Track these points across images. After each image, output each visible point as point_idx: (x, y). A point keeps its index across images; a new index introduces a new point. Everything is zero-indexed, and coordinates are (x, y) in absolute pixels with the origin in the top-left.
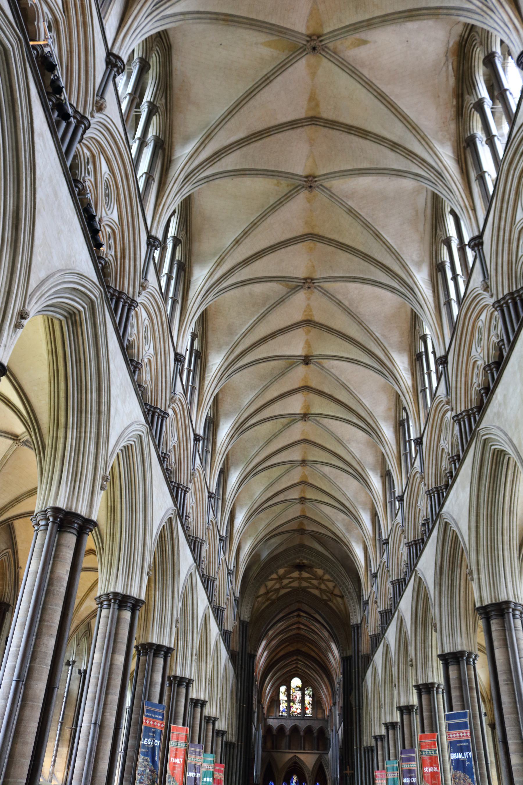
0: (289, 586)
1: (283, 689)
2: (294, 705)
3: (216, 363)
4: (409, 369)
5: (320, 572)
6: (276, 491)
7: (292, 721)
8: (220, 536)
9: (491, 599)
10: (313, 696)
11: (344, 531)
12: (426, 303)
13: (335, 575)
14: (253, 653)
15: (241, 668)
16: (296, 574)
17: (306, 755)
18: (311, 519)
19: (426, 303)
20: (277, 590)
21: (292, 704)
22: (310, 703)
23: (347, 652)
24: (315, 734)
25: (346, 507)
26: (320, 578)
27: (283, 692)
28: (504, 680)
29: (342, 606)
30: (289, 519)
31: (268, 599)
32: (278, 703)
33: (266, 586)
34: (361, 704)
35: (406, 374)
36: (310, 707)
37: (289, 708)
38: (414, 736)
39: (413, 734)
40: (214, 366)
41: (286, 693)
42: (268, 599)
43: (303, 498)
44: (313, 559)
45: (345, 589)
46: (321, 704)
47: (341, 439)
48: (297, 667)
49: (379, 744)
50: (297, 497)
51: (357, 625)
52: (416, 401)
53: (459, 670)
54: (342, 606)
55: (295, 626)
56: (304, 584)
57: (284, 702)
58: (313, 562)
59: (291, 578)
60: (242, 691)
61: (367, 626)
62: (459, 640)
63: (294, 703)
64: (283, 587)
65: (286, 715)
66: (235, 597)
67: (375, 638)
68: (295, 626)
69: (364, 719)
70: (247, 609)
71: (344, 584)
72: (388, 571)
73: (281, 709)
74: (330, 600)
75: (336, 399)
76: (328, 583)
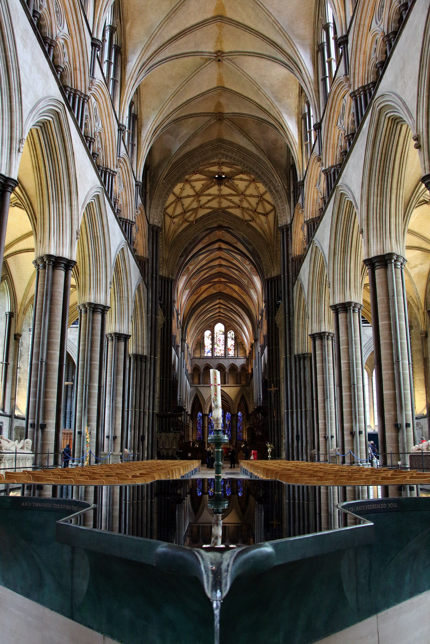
0: (207, 205)
5: (241, 185)
6: (182, 28)
8: (93, 39)
11: (272, 99)
13: (260, 173)
15: (152, 277)
16: (214, 190)
17: (229, 388)
18: (231, 90)
20: (195, 210)
21: (216, 346)
24: (239, 370)
25: (278, 45)
26: (242, 194)
29: (266, 225)
30: (203, 91)
31: (185, 220)
32: (204, 346)
33: (183, 205)
34: (292, 312)
37: (213, 350)
38: (394, 296)
39: (391, 294)
41: (211, 337)
42: (186, 220)
43: (219, 51)
45: (272, 188)
46: (243, 345)
48: (219, 312)
49: (318, 343)
50: (212, 51)
51: (286, 225)
54: (266, 225)
55: (216, 263)
56: (225, 204)
58: (234, 160)
59: (209, 195)
60: (154, 301)
61: (303, 212)
64: (201, 207)
66: (136, 181)
67: (312, 223)
68: (216, 263)
69: (296, 325)
70: (156, 212)
71: (271, 181)
73: (207, 350)
74: (253, 220)
76: (250, 199)
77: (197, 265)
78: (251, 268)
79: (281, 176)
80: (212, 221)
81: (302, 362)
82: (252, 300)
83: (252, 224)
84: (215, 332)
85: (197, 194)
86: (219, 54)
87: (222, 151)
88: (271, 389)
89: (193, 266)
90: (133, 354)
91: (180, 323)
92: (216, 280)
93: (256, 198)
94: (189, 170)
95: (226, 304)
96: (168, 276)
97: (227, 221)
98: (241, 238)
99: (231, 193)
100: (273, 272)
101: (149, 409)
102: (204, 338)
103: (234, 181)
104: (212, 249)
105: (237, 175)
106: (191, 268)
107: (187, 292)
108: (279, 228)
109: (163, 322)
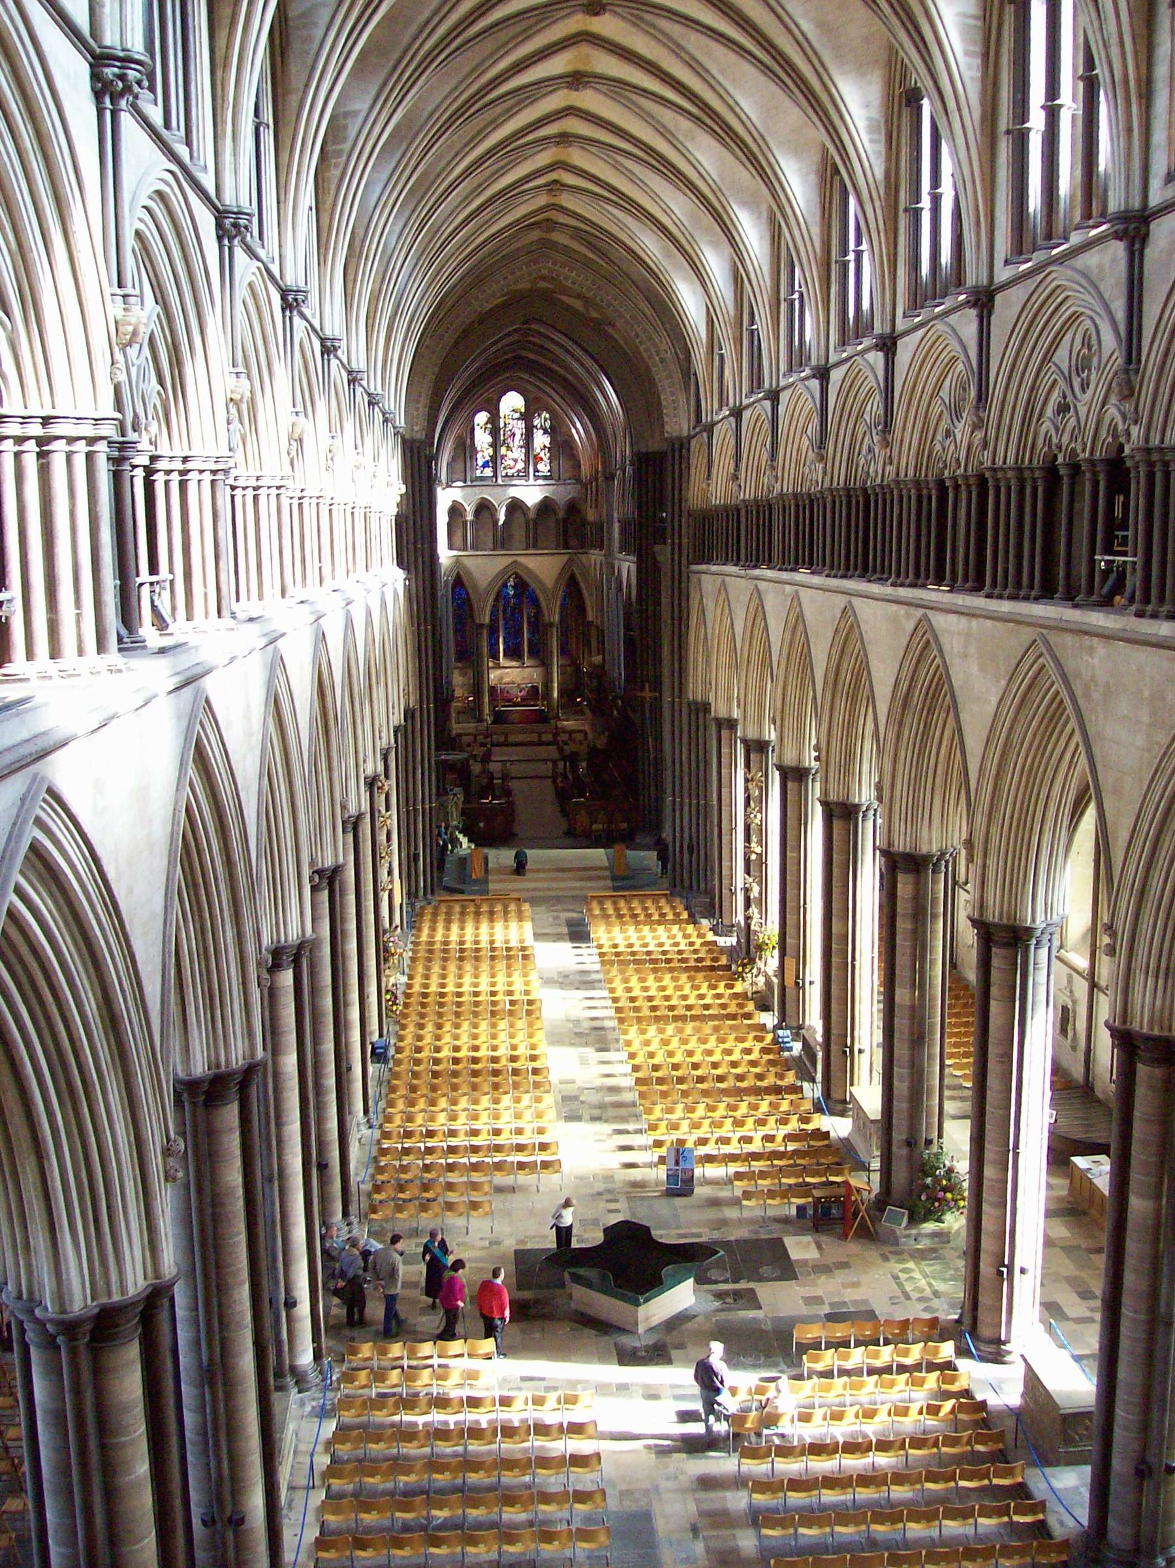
1: (482, 418)
2: (509, 453)
3: (355, 114)
4: (883, 121)
9: (1001, 914)
10: (552, 431)
12: (959, 110)
17: (539, 558)
19: (959, 110)
21: (503, 450)
24: (561, 514)
27: (482, 424)
28: (998, 1055)
32: (474, 451)
35: (871, 141)
36: (544, 455)
40: (349, 121)
45: (653, 351)
47: (672, 129)
51: (679, 438)
52: (889, 224)
53: (917, 883)
62: (925, 833)
63: (509, 448)
70: (417, 409)
71: (651, 339)
72: (773, 468)
73: (480, 463)
75: (667, 74)
79: (671, 334)
81: (701, 716)
83: (610, 330)
84: (502, 415)
86: (555, 187)
88: (643, 694)
101: (423, 803)
102: (473, 430)
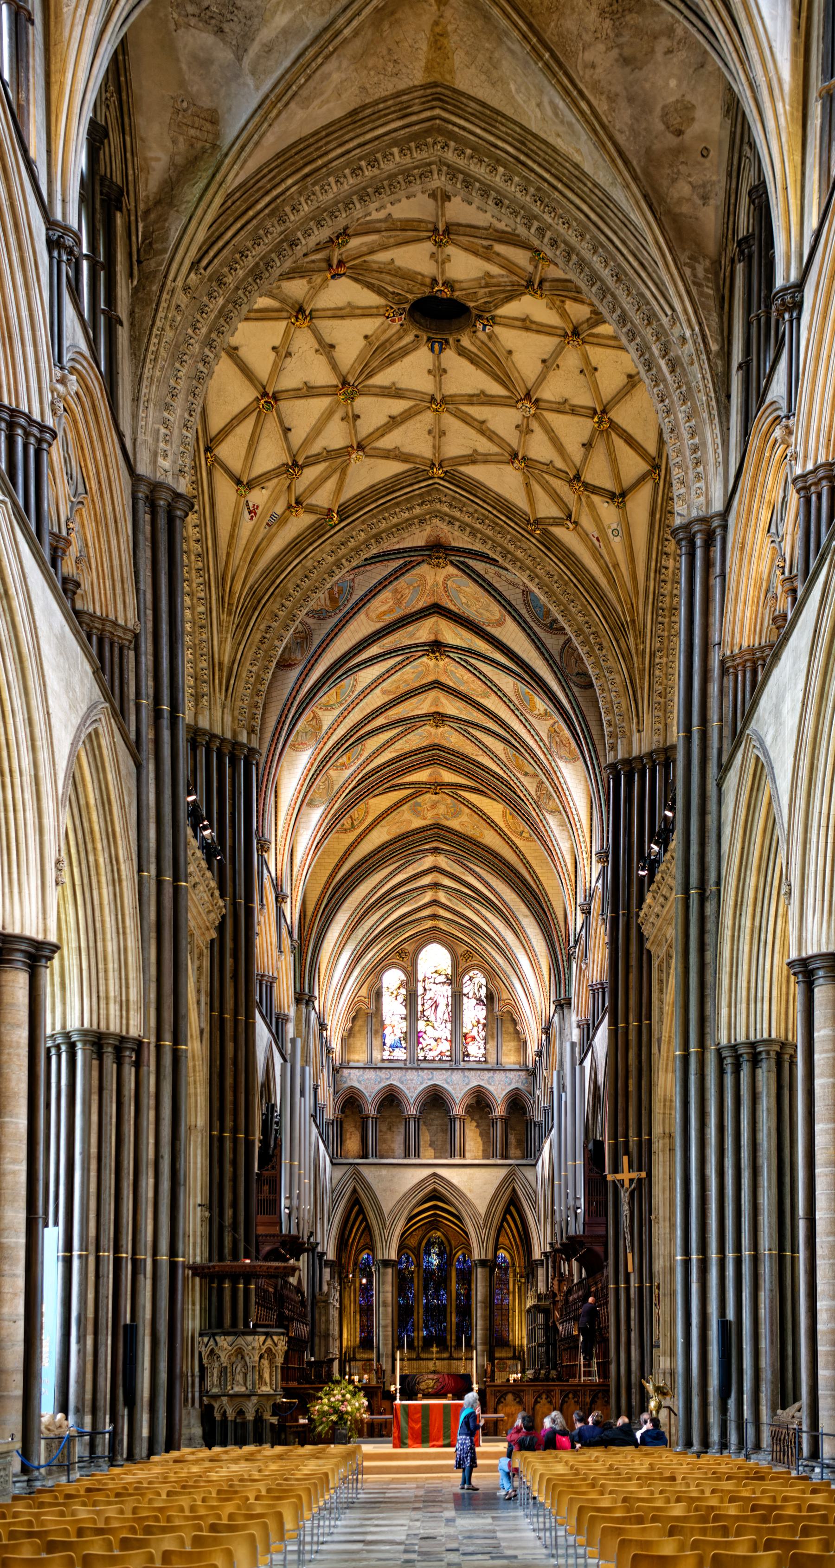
1: (393, 978)
2: (429, 1029)
7: (424, 1074)
14: (243, 738)
21: (421, 1025)
22: (478, 1022)
23: (630, 743)
37: (413, 1037)
41: (403, 991)
44: (498, 180)
46: (514, 1022)
48: (435, 902)
57: (398, 1018)
65: (403, 1057)
73: (389, 1041)
74: (569, 516)
77: (348, 710)
78: (553, 732)
80: (406, 515)
82: (551, 855)
84: (420, 977)
85: (345, 383)
87: (450, 156)
89: (337, 712)
90: (84, 1033)
91: (290, 933)
92: (422, 776)
93: (582, 419)
94: (307, 234)
95: (458, 870)
96: (235, 733)
97: (467, 519)
98: (515, 597)
99: (483, 392)
100: (636, 736)
102: (379, 995)
103: (497, 329)
104: (409, 647)
105: (509, 299)
106: (328, 719)
107: (315, 816)
108: (674, 533)
109: (215, 917)
